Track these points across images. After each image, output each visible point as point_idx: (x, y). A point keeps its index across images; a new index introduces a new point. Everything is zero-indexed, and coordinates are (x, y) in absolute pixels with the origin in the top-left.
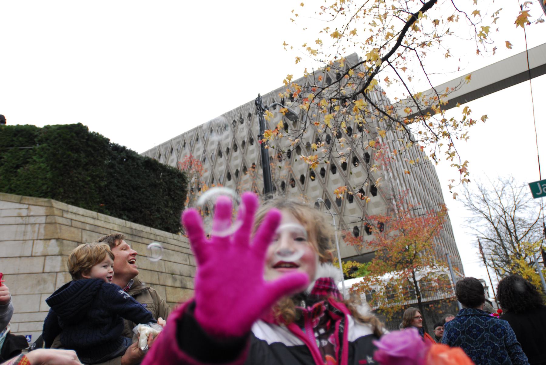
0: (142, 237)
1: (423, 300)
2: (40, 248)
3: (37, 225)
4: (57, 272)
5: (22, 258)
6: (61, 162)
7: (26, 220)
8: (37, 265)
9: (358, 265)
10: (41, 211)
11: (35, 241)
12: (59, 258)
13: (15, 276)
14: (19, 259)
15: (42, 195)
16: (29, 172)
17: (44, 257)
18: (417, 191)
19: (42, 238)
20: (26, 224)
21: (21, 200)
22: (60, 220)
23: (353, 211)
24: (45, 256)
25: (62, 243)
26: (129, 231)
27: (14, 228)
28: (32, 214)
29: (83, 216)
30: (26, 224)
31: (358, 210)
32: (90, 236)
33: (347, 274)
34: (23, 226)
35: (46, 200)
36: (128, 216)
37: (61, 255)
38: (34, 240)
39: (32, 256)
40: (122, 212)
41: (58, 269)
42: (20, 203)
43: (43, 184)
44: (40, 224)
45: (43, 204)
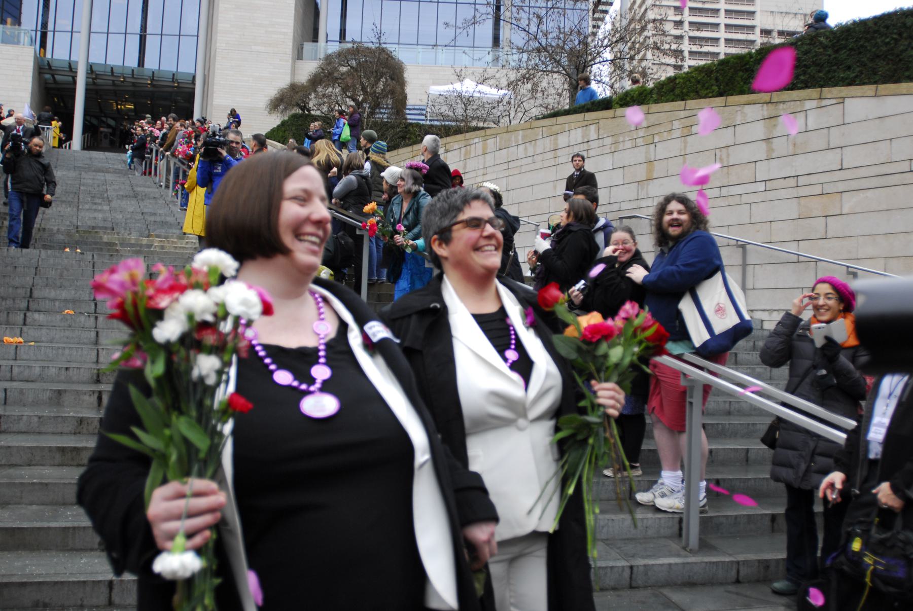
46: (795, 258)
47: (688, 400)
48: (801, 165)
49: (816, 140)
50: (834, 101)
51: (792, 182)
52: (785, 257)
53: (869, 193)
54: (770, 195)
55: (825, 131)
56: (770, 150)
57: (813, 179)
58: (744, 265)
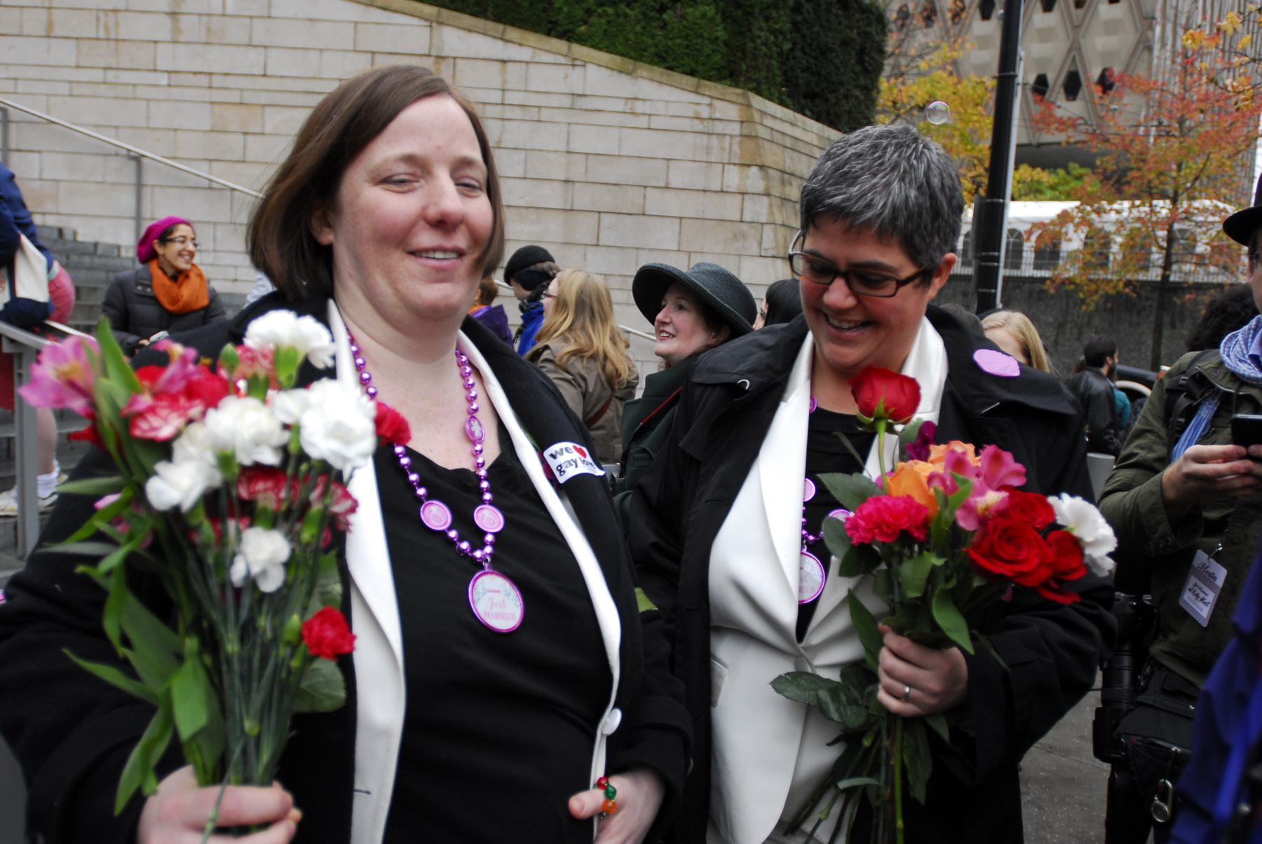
1: (1173, 278)
2: (733, 178)
3: (728, 138)
7: (708, 126)
8: (730, 208)
9: (1044, 177)
10: (732, 111)
11: (727, 167)
12: (765, 200)
15: (713, 73)
16: (685, 23)
17: (740, 197)
19: (737, 161)
20: (709, 134)
21: (698, 86)
22: (762, 132)
24: (743, 194)
25: (767, 173)
27: (690, 138)
28: (717, 115)
30: (709, 134)
31: (1061, 32)
32: (792, 159)
33: (1016, 196)
34: (705, 137)
35: (739, 91)
36: (811, 110)
37: (768, 195)
40: (803, 101)
41: (763, 219)
44: (731, 136)
46: (206, 184)
47: (16, 371)
48: (217, 59)
49: (236, 32)
51: (204, 81)
52: (193, 181)
54: (175, 93)
55: (247, 21)
56: (177, 30)
57: (231, 82)
58: (139, 186)
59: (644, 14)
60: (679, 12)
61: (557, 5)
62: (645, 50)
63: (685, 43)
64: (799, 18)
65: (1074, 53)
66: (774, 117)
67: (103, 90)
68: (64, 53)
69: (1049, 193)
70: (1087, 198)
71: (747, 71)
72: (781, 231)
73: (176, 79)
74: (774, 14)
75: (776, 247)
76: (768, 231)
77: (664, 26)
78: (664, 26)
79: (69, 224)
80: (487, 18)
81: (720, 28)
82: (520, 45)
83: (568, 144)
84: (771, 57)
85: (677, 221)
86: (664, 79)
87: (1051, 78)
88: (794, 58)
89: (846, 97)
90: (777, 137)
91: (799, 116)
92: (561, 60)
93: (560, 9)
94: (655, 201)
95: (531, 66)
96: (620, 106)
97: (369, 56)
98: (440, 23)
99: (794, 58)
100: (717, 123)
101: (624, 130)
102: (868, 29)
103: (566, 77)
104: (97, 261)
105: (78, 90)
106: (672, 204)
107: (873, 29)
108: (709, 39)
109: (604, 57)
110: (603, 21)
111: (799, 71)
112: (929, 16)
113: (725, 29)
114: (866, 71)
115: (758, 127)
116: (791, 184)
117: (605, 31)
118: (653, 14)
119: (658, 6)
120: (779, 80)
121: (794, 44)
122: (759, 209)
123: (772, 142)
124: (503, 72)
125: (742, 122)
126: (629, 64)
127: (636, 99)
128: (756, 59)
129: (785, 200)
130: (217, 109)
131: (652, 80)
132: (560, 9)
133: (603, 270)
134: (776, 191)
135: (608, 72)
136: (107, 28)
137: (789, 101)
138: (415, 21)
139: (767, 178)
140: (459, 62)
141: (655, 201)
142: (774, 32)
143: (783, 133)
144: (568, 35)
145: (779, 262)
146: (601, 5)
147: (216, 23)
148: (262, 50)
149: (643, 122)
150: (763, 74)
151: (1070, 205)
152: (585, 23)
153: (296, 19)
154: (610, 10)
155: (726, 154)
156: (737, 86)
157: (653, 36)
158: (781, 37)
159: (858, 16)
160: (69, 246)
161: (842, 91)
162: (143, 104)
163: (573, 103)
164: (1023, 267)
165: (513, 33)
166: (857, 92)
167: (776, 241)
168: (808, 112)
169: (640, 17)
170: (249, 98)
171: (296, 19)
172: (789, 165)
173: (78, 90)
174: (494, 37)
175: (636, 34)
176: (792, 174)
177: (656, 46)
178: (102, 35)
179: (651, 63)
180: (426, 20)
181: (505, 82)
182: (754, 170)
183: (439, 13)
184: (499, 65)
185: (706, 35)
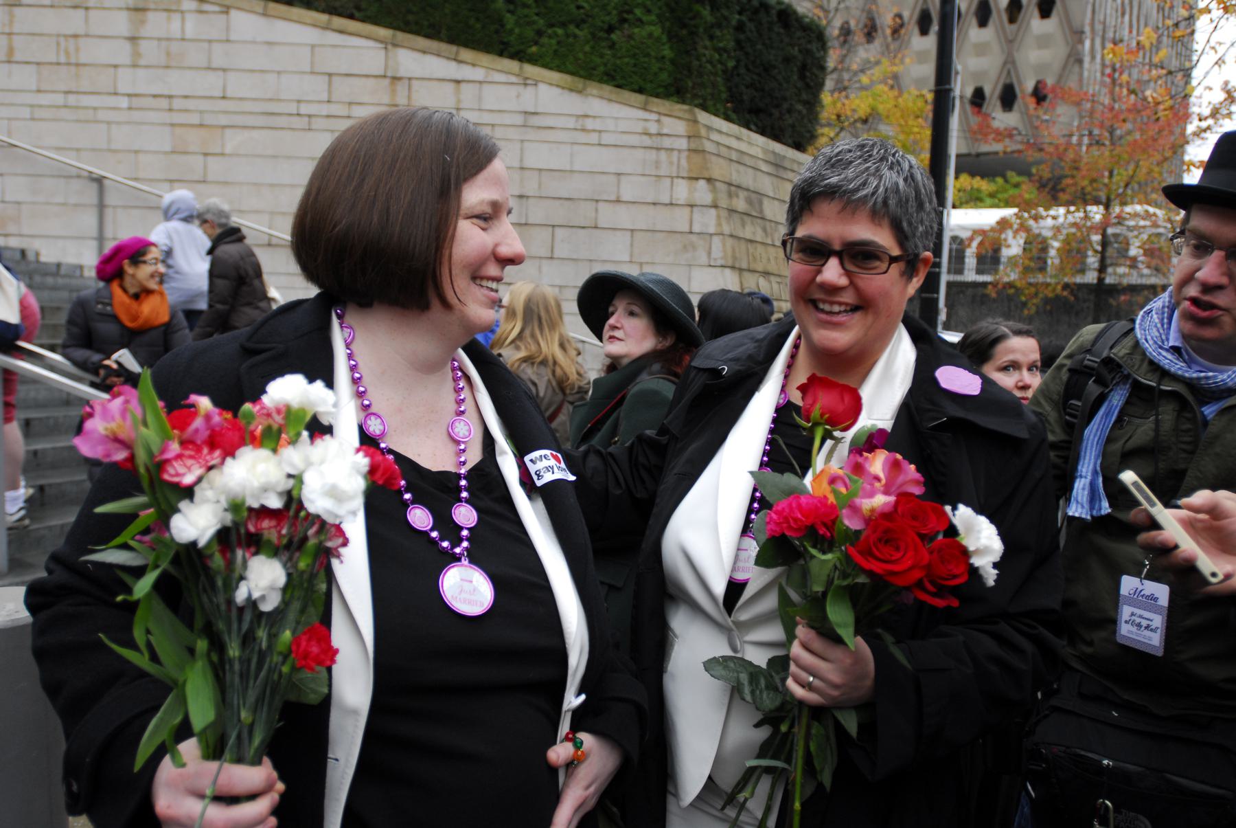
0: (785, 169)
1: (1109, 280)
2: (682, 191)
3: (675, 153)
4: (711, 235)
5: (658, 207)
6: (684, 26)
8: (680, 220)
10: (680, 127)
11: (675, 180)
12: (713, 211)
13: (649, 234)
14: (652, 207)
15: (661, 90)
17: (688, 210)
18: (1144, 11)
19: (685, 175)
20: (658, 149)
21: (646, 103)
22: (709, 147)
23: (981, 49)
24: (691, 206)
26: (772, 159)
27: (639, 153)
28: (665, 131)
29: (727, 134)
30: (658, 149)
32: (738, 172)
34: (654, 152)
35: (686, 107)
36: (756, 125)
37: (716, 206)
38: (672, 178)
39: (672, 204)
40: (747, 116)
41: (712, 230)
42: (645, 109)
43: (661, 69)
44: (679, 151)
45: (680, 114)
48: (176, 82)
50: (217, 8)
51: (164, 103)
53: (255, 134)
54: (136, 116)
55: (206, 45)
56: (136, 54)
57: (190, 104)
58: (101, 207)
59: (593, 35)
60: (626, 32)
61: (508, 27)
62: (594, 69)
63: (633, 61)
64: (742, 37)
65: (1009, 66)
66: (720, 132)
67: (64, 113)
68: (24, 77)
69: (989, 201)
70: (1025, 206)
71: (693, 88)
72: (730, 242)
73: (136, 102)
74: (718, 33)
75: (724, 257)
76: (716, 241)
77: (612, 46)
78: (612, 46)
79: (32, 245)
80: (441, 40)
81: (667, 47)
82: (474, 65)
83: (521, 160)
84: (716, 74)
85: (629, 233)
86: (613, 97)
87: (987, 90)
88: (738, 75)
89: (789, 111)
90: (724, 151)
91: (744, 131)
92: (513, 79)
93: (511, 31)
94: (607, 215)
95: (485, 86)
96: (571, 123)
97: (326, 78)
98: (395, 45)
99: (738, 75)
100: (665, 138)
101: (576, 147)
102: (809, 46)
103: (518, 96)
104: (60, 281)
105: (39, 113)
106: (623, 217)
107: (813, 47)
108: (656, 58)
109: (555, 76)
110: (554, 42)
111: (743, 88)
112: (871, 32)
113: (671, 48)
114: (808, 86)
115: (705, 141)
116: (737, 196)
117: (556, 51)
118: (602, 34)
119: (606, 27)
120: (724, 96)
121: (738, 61)
122: (707, 221)
123: (718, 155)
124: (458, 92)
125: (689, 137)
126: (579, 82)
127: (587, 116)
128: (701, 75)
129: (732, 211)
130: (178, 130)
131: (601, 97)
132: (511, 31)
133: (558, 282)
134: (724, 203)
135: (559, 91)
136: (67, 53)
137: (734, 116)
138: (371, 43)
139: (714, 190)
140: (414, 83)
141: (607, 215)
142: (718, 50)
143: (729, 147)
144: (519, 55)
145: (728, 271)
146: (552, 26)
147: (175, 47)
148: (220, 73)
149: (594, 138)
150: (709, 90)
151: (1009, 212)
152: (536, 43)
153: (254, 42)
154: (560, 31)
155: (675, 168)
156: (684, 102)
157: (602, 56)
158: (725, 55)
159: (799, 34)
160: (32, 266)
161: (785, 106)
162: (104, 126)
163: (525, 121)
164: (966, 272)
165: (466, 54)
166: (799, 107)
167: (725, 251)
168: (753, 127)
169: (589, 37)
170: (209, 120)
171: (254, 42)
172: (735, 178)
173: (39, 113)
174: (448, 58)
175: (585, 53)
176: (738, 187)
177: (605, 65)
178: (63, 59)
179: (601, 81)
180: (381, 42)
181: (459, 101)
182: (702, 183)
183: (394, 36)
184: (452, 86)
185: (653, 54)
